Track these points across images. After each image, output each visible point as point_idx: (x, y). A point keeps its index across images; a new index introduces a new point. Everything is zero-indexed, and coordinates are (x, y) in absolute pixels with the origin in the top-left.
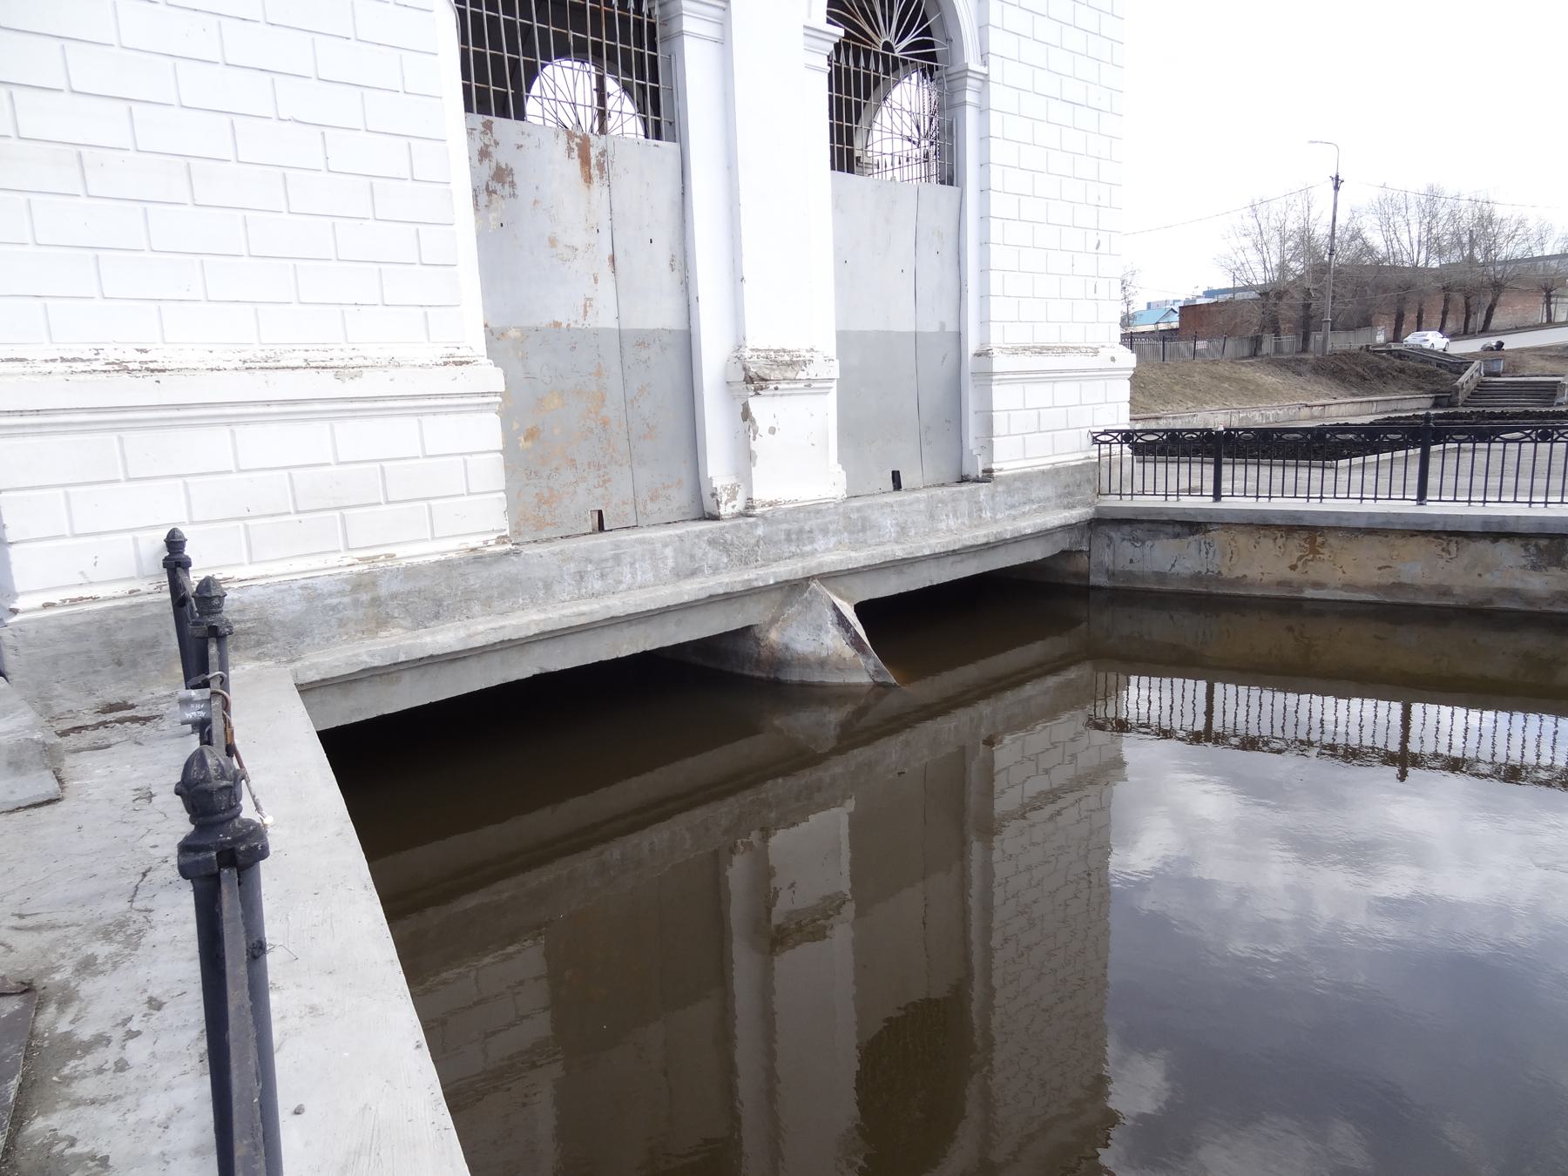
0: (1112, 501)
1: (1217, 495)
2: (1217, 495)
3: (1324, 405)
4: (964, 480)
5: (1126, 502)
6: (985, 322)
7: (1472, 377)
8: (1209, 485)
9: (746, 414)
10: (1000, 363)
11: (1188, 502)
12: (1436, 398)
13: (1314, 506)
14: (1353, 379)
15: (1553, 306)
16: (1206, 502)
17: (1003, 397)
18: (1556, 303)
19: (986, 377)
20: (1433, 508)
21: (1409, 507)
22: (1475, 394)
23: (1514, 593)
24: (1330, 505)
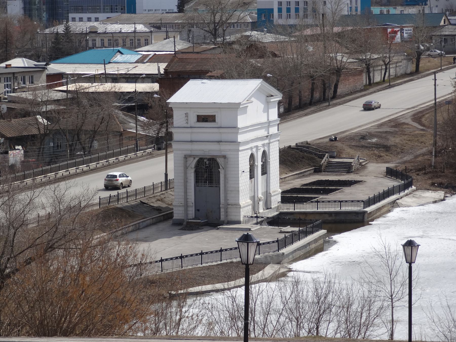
0: (281, 211)
1: (294, 210)
2: (294, 210)
3: (285, 178)
4: (268, 209)
5: (283, 211)
6: (270, 189)
7: (326, 160)
8: (293, 208)
9: (259, 203)
10: (272, 194)
11: (291, 211)
12: (315, 169)
13: (306, 211)
14: (289, 163)
15: (371, 75)
16: (293, 210)
17: (272, 198)
18: (374, 71)
19: (271, 196)
20: (319, 210)
21: (315, 210)
22: (326, 167)
23: (327, 220)
24: (308, 210)
